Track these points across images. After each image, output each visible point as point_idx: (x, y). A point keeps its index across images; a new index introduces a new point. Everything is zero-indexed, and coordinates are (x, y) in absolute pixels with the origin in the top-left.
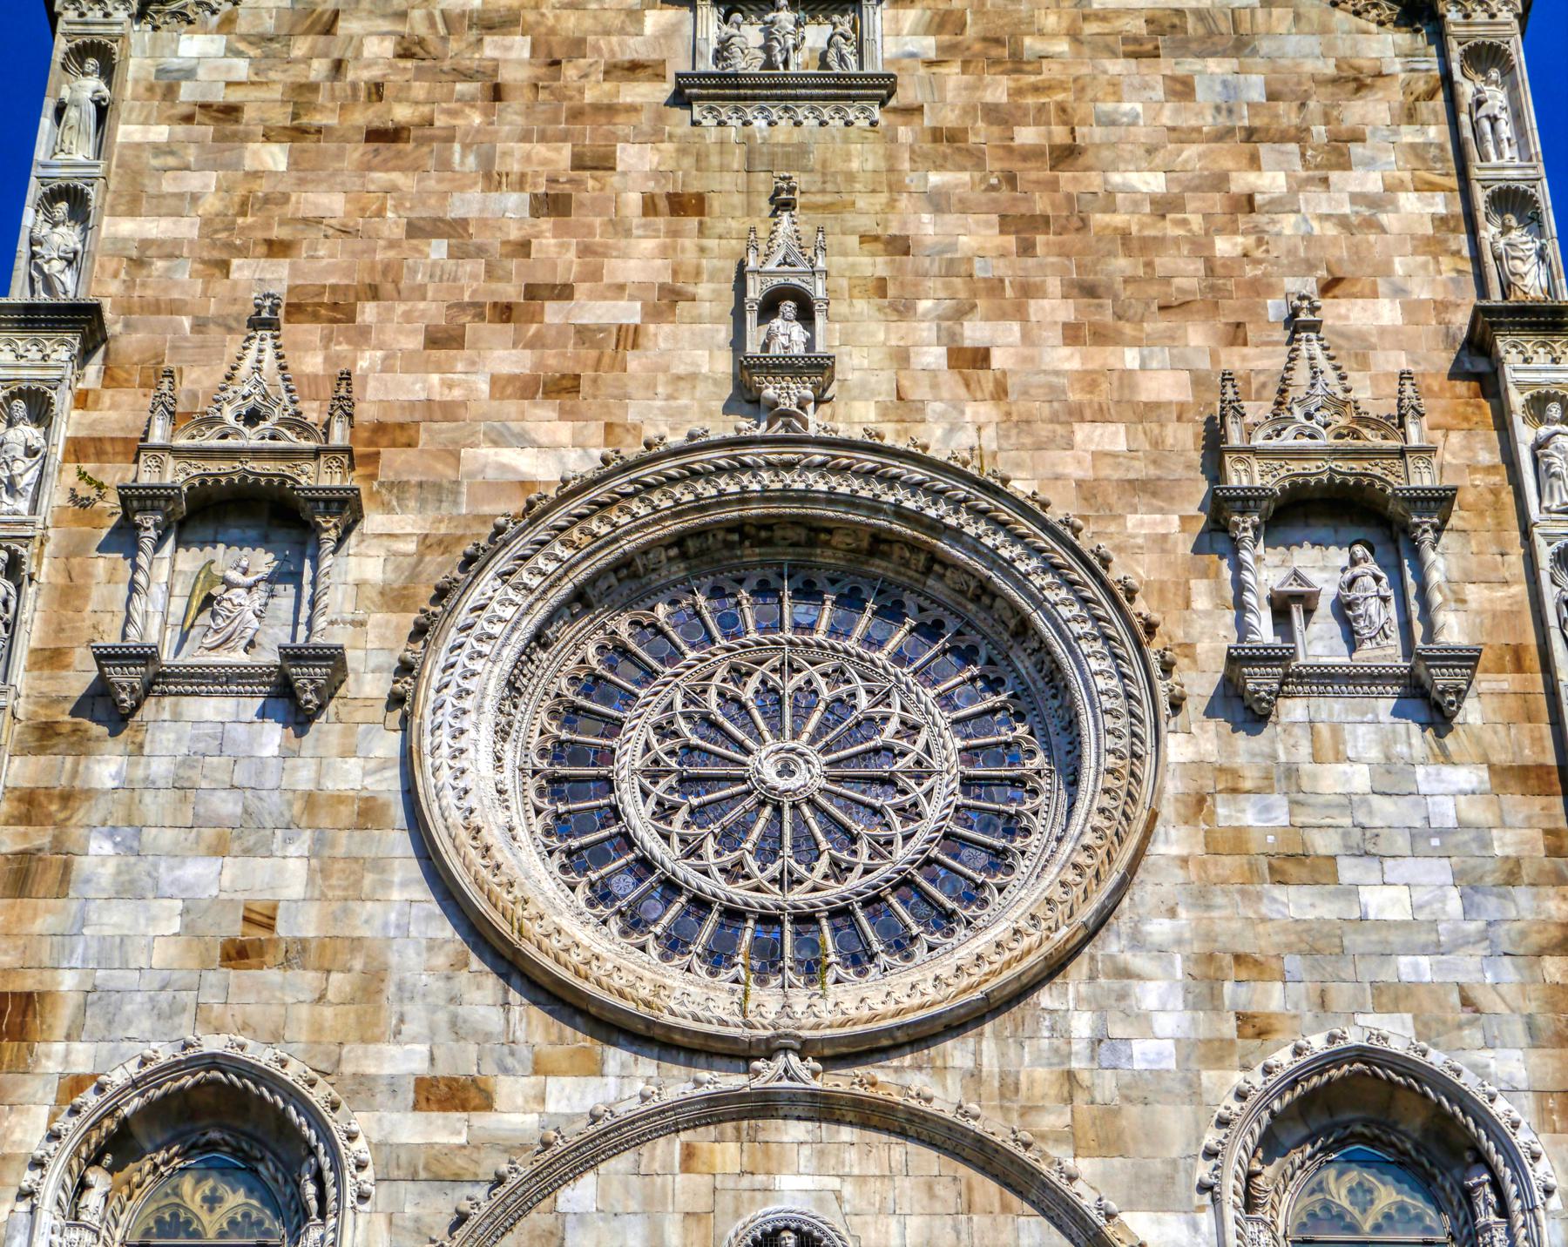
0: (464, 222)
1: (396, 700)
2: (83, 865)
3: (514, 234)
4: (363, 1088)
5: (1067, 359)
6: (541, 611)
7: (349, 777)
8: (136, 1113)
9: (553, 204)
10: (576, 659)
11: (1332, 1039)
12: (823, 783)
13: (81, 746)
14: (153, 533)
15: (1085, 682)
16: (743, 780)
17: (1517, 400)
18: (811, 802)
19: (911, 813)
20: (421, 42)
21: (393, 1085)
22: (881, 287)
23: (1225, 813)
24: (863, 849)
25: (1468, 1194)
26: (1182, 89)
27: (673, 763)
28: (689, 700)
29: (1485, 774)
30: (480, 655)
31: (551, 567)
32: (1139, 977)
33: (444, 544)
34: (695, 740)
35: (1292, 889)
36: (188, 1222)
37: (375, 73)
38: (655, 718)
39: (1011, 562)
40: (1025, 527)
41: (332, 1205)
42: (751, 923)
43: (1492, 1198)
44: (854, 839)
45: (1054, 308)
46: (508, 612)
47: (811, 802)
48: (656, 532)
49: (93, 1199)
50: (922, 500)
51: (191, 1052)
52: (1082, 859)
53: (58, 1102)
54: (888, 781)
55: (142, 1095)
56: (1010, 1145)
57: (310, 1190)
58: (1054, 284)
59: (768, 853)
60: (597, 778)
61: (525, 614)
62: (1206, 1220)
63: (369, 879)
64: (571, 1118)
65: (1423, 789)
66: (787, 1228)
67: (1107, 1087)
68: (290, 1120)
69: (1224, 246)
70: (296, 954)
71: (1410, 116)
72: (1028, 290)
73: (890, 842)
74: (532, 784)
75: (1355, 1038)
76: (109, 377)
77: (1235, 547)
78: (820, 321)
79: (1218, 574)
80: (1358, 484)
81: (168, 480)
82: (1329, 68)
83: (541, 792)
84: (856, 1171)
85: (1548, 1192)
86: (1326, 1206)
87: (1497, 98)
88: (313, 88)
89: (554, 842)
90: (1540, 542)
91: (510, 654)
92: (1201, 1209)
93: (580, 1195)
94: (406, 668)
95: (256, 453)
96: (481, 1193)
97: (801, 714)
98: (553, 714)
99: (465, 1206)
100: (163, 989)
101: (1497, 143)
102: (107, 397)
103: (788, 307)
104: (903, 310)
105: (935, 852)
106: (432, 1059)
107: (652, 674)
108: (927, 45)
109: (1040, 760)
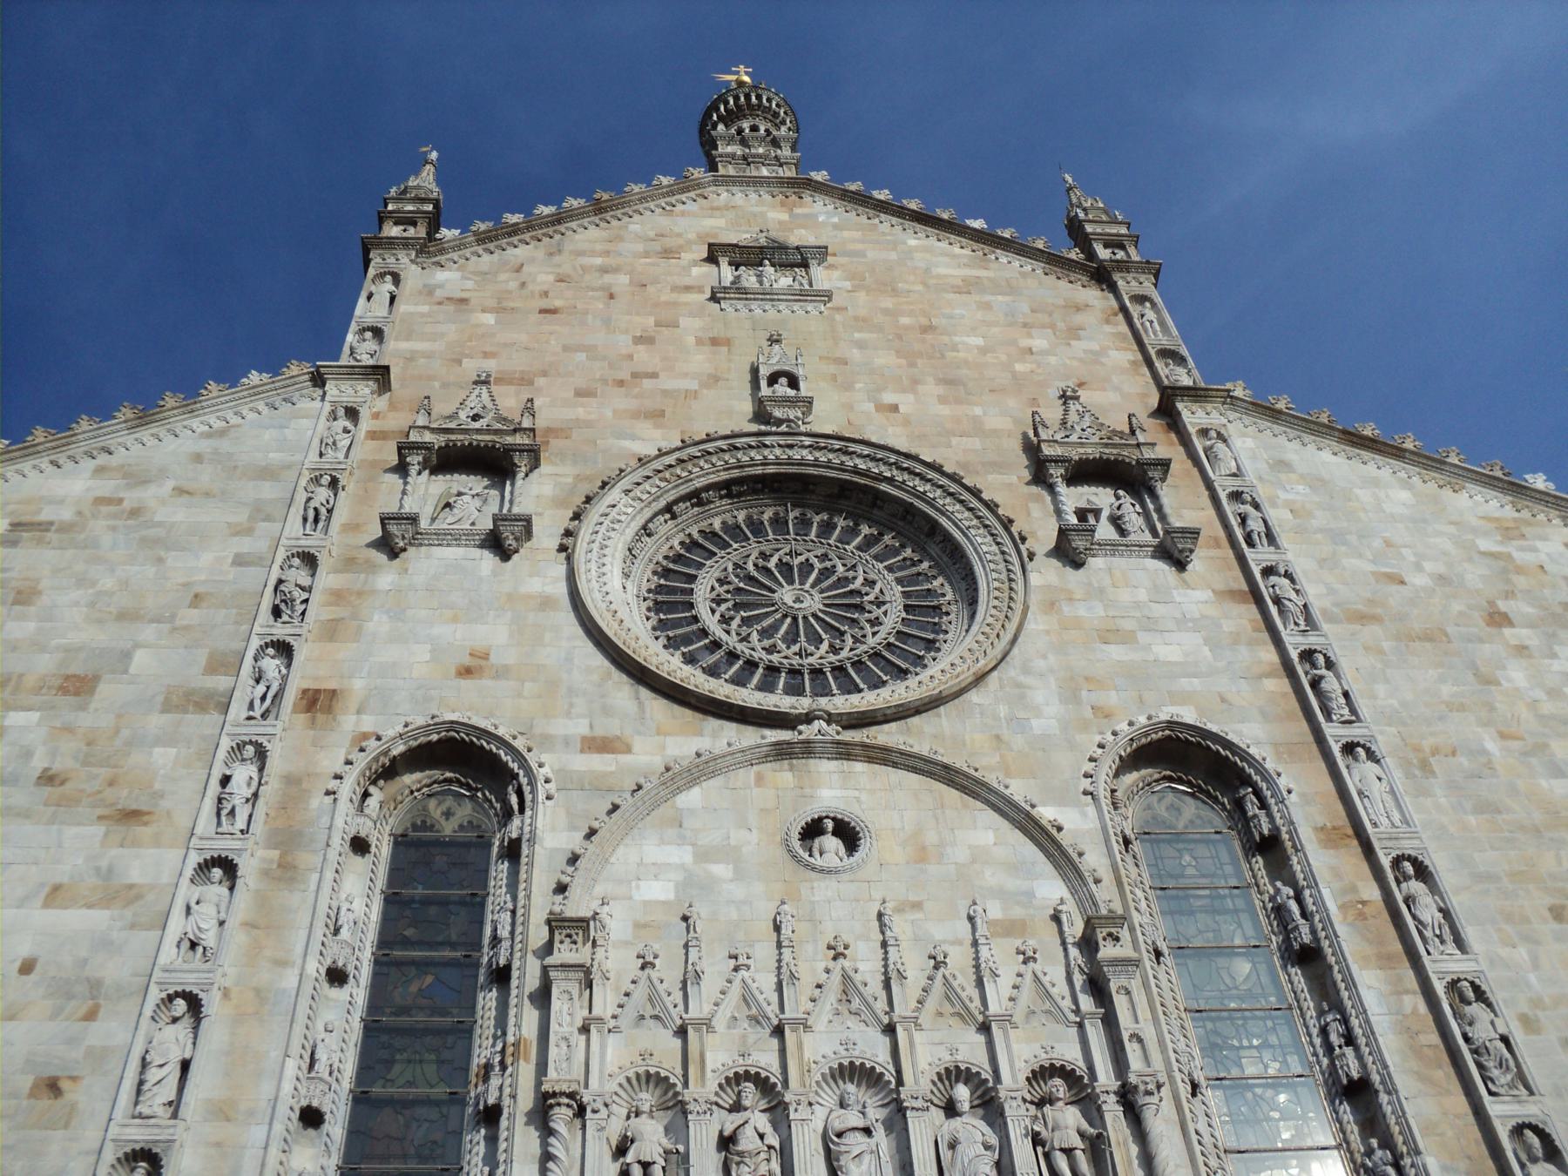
0: (595, 346)
1: (563, 548)
2: (370, 627)
3: (624, 351)
4: (547, 741)
5: (945, 410)
6: (648, 513)
7: (535, 586)
8: (402, 755)
9: (644, 340)
10: (666, 547)
11: (1149, 718)
12: (821, 607)
13: (372, 568)
14: (417, 467)
15: (975, 549)
16: (773, 605)
17: (1192, 430)
18: (815, 616)
19: (875, 622)
20: (569, 276)
21: (567, 741)
22: (834, 378)
23: (1066, 609)
24: (849, 641)
25: (1239, 804)
26: (987, 306)
27: (729, 596)
28: (736, 566)
29: (1211, 594)
30: (614, 530)
31: (654, 490)
32: (1030, 688)
33: (588, 479)
34: (742, 585)
35: (1112, 646)
36: (433, 826)
37: (545, 288)
38: (717, 574)
39: (924, 493)
40: (931, 475)
41: (528, 803)
42: (783, 674)
43: (1255, 800)
44: (842, 633)
45: (931, 389)
46: (630, 510)
47: (815, 616)
48: (713, 478)
49: (373, 803)
50: (871, 464)
51: (436, 720)
52: (987, 630)
53: (352, 745)
54: (860, 608)
55: (405, 743)
56: (966, 769)
57: (514, 800)
58: (930, 379)
59: (792, 638)
60: (683, 603)
61: (639, 512)
62: (1091, 811)
63: (548, 637)
64: (683, 758)
65: (1178, 599)
66: (827, 817)
67: (1018, 742)
68: (501, 760)
69: (1019, 367)
70: (502, 673)
71: (1108, 322)
72: (915, 382)
73: (864, 636)
74: (644, 605)
75: (1164, 717)
76: (392, 406)
77: (1051, 488)
78: (802, 385)
79: (1043, 501)
80: (1116, 460)
81: (427, 440)
82: (1062, 302)
83: (649, 609)
84: (868, 787)
85: (1289, 792)
86: (1154, 818)
87: (1150, 315)
88: (510, 292)
89: (658, 633)
90: (1219, 490)
91: (630, 533)
92: (1087, 805)
93: (692, 798)
94: (568, 533)
95: (478, 431)
96: (628, 795)
97: (804, 577)
98: (655, 573)
99: (618, 801)
100: (418, 689)
101: (1155, 334)
102: (391, 415)
103: (783, 380)
104: (848, 387)
105: (892, 640)
106: (591, 727)
107: (715, 554)
108: (848, 285)
109: (949, 597)
